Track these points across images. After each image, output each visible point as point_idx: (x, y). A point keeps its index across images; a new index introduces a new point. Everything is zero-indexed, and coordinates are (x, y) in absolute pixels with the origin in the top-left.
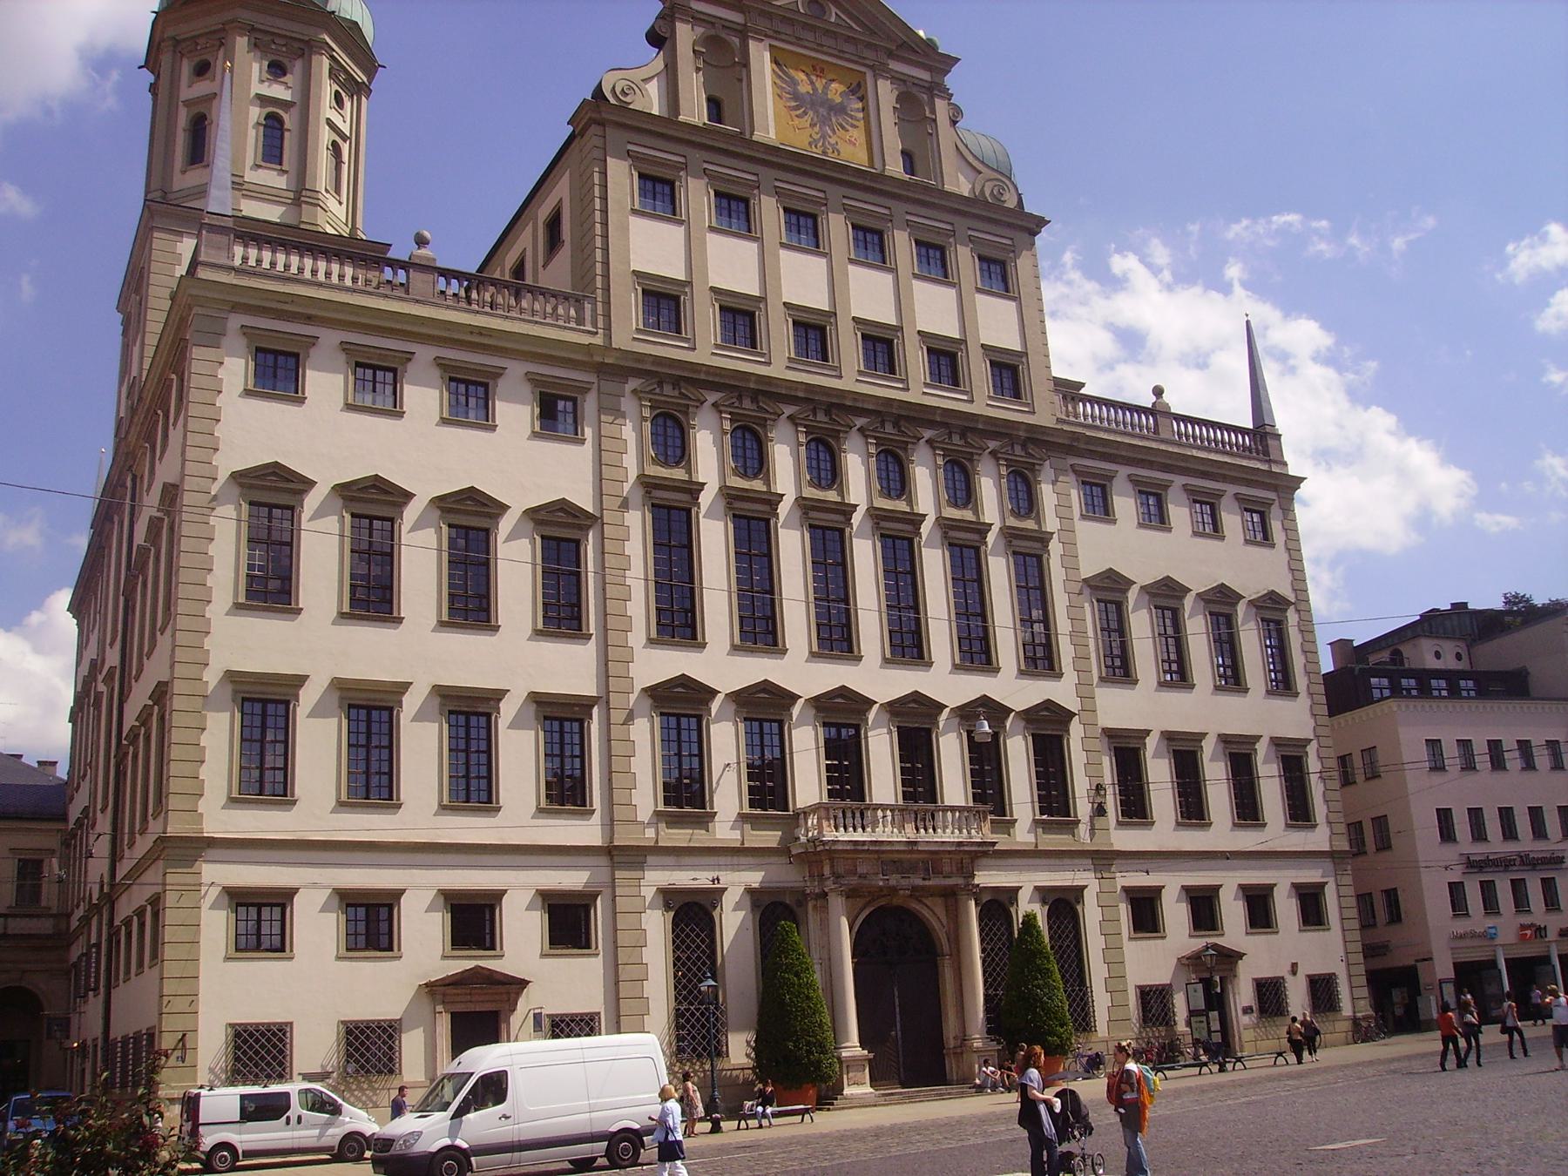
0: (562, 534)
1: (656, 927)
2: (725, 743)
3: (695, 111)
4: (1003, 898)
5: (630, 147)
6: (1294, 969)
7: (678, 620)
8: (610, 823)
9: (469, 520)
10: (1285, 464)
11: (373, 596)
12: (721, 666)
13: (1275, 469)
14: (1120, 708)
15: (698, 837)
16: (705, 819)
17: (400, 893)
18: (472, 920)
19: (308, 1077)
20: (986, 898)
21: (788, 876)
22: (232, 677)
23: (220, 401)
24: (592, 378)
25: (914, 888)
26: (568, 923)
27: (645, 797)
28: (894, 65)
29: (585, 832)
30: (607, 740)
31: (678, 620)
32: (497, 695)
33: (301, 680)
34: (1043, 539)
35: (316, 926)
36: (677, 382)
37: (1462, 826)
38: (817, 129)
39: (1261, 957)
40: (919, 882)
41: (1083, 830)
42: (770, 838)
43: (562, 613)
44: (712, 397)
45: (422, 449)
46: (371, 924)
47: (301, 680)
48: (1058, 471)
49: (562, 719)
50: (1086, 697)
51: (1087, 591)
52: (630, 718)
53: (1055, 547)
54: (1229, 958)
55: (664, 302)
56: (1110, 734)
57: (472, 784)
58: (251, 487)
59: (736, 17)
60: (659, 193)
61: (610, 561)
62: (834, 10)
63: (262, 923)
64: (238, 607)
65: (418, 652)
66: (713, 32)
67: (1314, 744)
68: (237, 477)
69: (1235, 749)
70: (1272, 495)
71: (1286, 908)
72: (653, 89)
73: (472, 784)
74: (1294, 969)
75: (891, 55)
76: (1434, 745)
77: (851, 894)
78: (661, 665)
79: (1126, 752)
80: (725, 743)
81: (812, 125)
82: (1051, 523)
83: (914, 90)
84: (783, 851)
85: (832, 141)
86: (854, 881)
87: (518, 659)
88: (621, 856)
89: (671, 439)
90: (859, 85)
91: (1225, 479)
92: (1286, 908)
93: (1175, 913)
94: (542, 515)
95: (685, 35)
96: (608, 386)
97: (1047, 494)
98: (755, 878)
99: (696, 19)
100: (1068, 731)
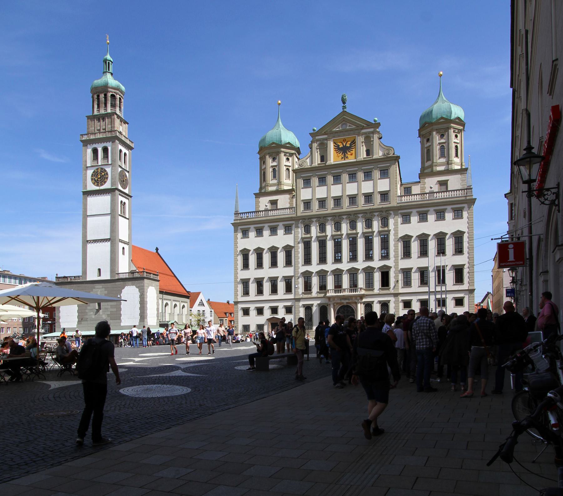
0: (288, 251)
2: (315, 281)
3: (317, 161)
7: (308, 261)
8: (295, 295)
11: (260, 265)
14: (405, 264)
15: (309, 296)
21: (324, 301)
22: (241, 279)
24: (293, 222)
25: (347, 303)
29: (291, 296)
30: (295, 282)
31: (308, 261)
32: (278, 277)
33: (250, 279)
41: (391, 289)
42: (322, 295)
43: (288, 263)
45: (266, 241)
47: (250, 279)
48: (396, 215)
51: (400, 240)
52: (299, 278)
55: (307, 204)
59: (325, 136)
60: (307, 183)
61: (296, 253)
62: (348, 124)
64: (242, 270)
65: (267, 272)
68: (240, 251)
72: (308, 160)
75: (362, 129)
78: (303, 269)
79: (407, 273)
80: (315, 281)
82: (391, 226)
84: (324, 297)
87: (281, 271)
88: (298, 300)
89: (307, 230)
95: (315, 145)
97: (391, 222)
98: (319, 302)
99: (317, 141)
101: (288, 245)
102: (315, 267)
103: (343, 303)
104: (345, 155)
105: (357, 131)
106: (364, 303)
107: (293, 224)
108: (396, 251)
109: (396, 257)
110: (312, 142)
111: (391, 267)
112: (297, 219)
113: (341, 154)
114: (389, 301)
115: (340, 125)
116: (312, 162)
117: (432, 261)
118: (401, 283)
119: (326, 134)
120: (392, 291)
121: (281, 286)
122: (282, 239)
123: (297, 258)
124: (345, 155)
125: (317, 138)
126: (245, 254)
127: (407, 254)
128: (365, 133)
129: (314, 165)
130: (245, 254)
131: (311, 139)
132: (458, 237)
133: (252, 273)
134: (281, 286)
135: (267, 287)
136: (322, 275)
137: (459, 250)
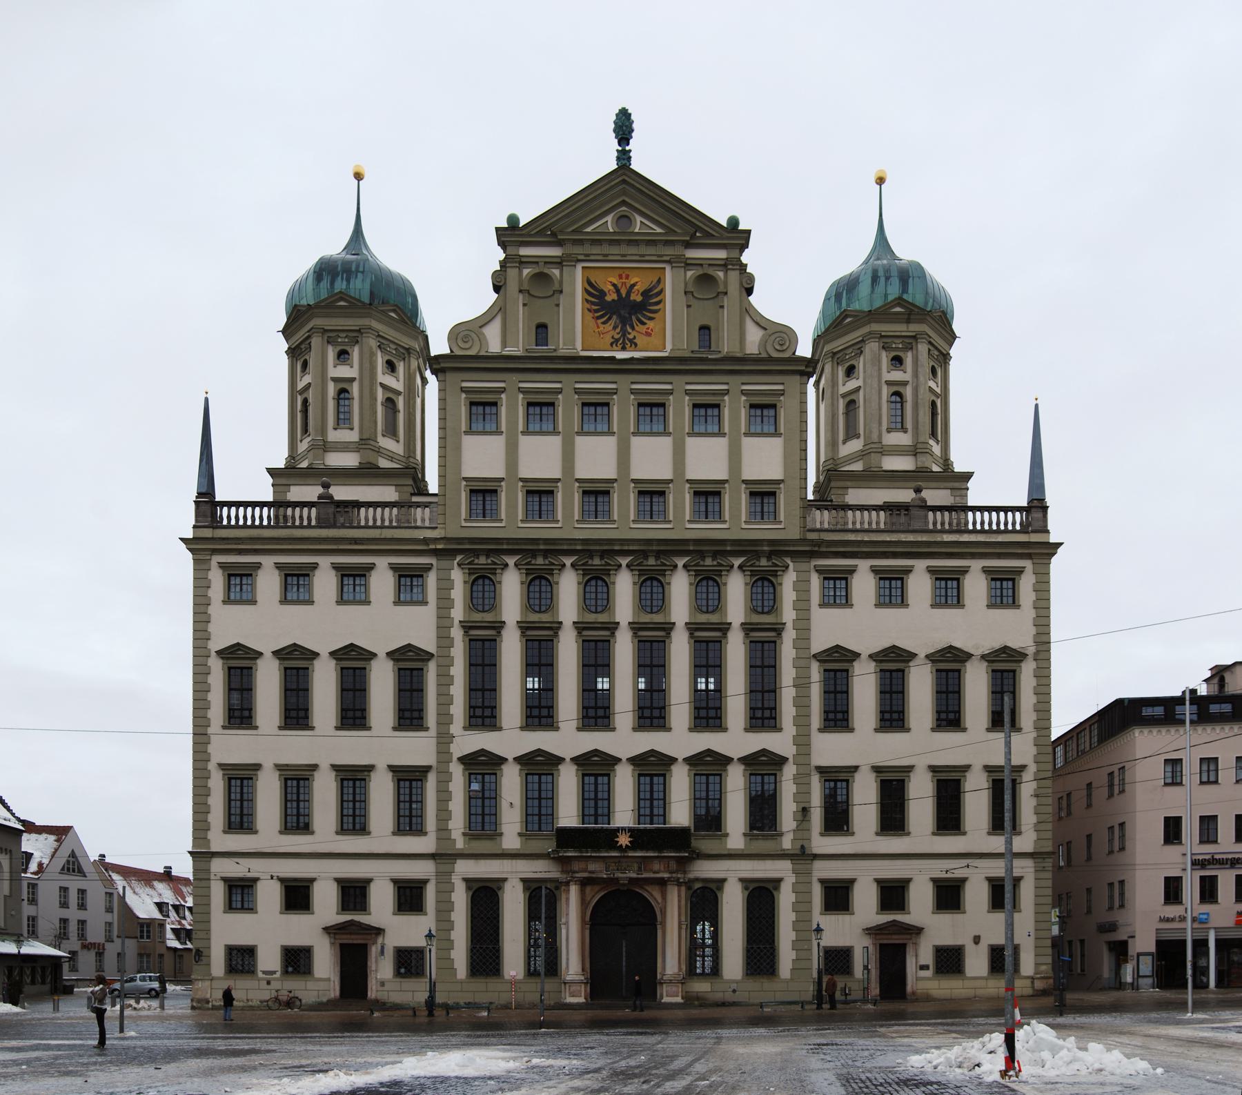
0: (410, 663)
1: (460, 899)
4: (713, 886)
5: (464, 384)
6: (977, 940)
7: (483, 713)
9: (353, 663)
10: (1048, 532)
11: (296, 715)
12: (511, 739)
13: (1035, 538)
14: (831, 749)
16: (496, 835)
17: (312, 880)
18: (354, 894)
19: (264, 972)
20: (697, 885)
22: (222, 766)
23: (211, 610)
24: (431, 560)
25: (631, 879)
26: (409, 897)
27: (457, 824)
28: (693, 254)
34: (778, 629)
35: (269, 895)
36: (488, 553)
37: (1190, 830)
38: (618, 330)
39: (941, 930)
40: (634, 875)
43: (409, 716)
44: (511, 561)
45: (324, 624)
46: (297, 896)
49: (409, 779)
50: (803, 742)
53: (789, 636)
54: (917, 931)
56: (822, 770)
57: (353, 819)
58: (228, 659)
59: (554, 252)
62: (639, 219)
63: (241, 893)
65: (325, 745)
66: (537, 271)
67: (1032, 768)
69: (943, 776)
70: (1027, 564)
71: (976, 894)
73: (353, 819)
74: (977, 940)
75: (688, 245)
76: (1174, 764)
77: (584, 883)
78: (468, 742)
79: (837, 780)
81: (615, 328)
82: (788, 615)
83: (711, 271)
85: (631, 337)
86: (585, 875)
87: (384, 745)
90: (659, 281)
91: (973, 556)
92: (976, 894)
93: (865, 899)
94: (397, 656)
96: (445, 563)
100: (781, 770)
101: (409, 647)
102: (511, 739)
103: (615, 881)
104: (624, 333)
105: (669, 251)
106: (689, 884)
107: (428, 568)
108: (802, 703)
109: (802, 720)
110: (503, 264)
111: (782, 760)
112: (447, 550)
113: (609, 327)
114: (777, 882)
115: (609, 218)
116: (504, 344)
117: (921, 747)
118: (817, 816)
119: (559, 243)
120: (787, 843)
121: (381, 798)
122: (387, 622)
123: (445, 700)
124: (624, 333)
125: (524, 251)
126: (239, 663)
127: (838, 717)
128: (698, 264)
129: (510, 351)
130: (239, 663)
131: (502, 256)
132: (1005, 667)
133: (267, 745)
134: (381, 798)
135: (325, 796)
136: (539, 766)
137: (1002, 718)
